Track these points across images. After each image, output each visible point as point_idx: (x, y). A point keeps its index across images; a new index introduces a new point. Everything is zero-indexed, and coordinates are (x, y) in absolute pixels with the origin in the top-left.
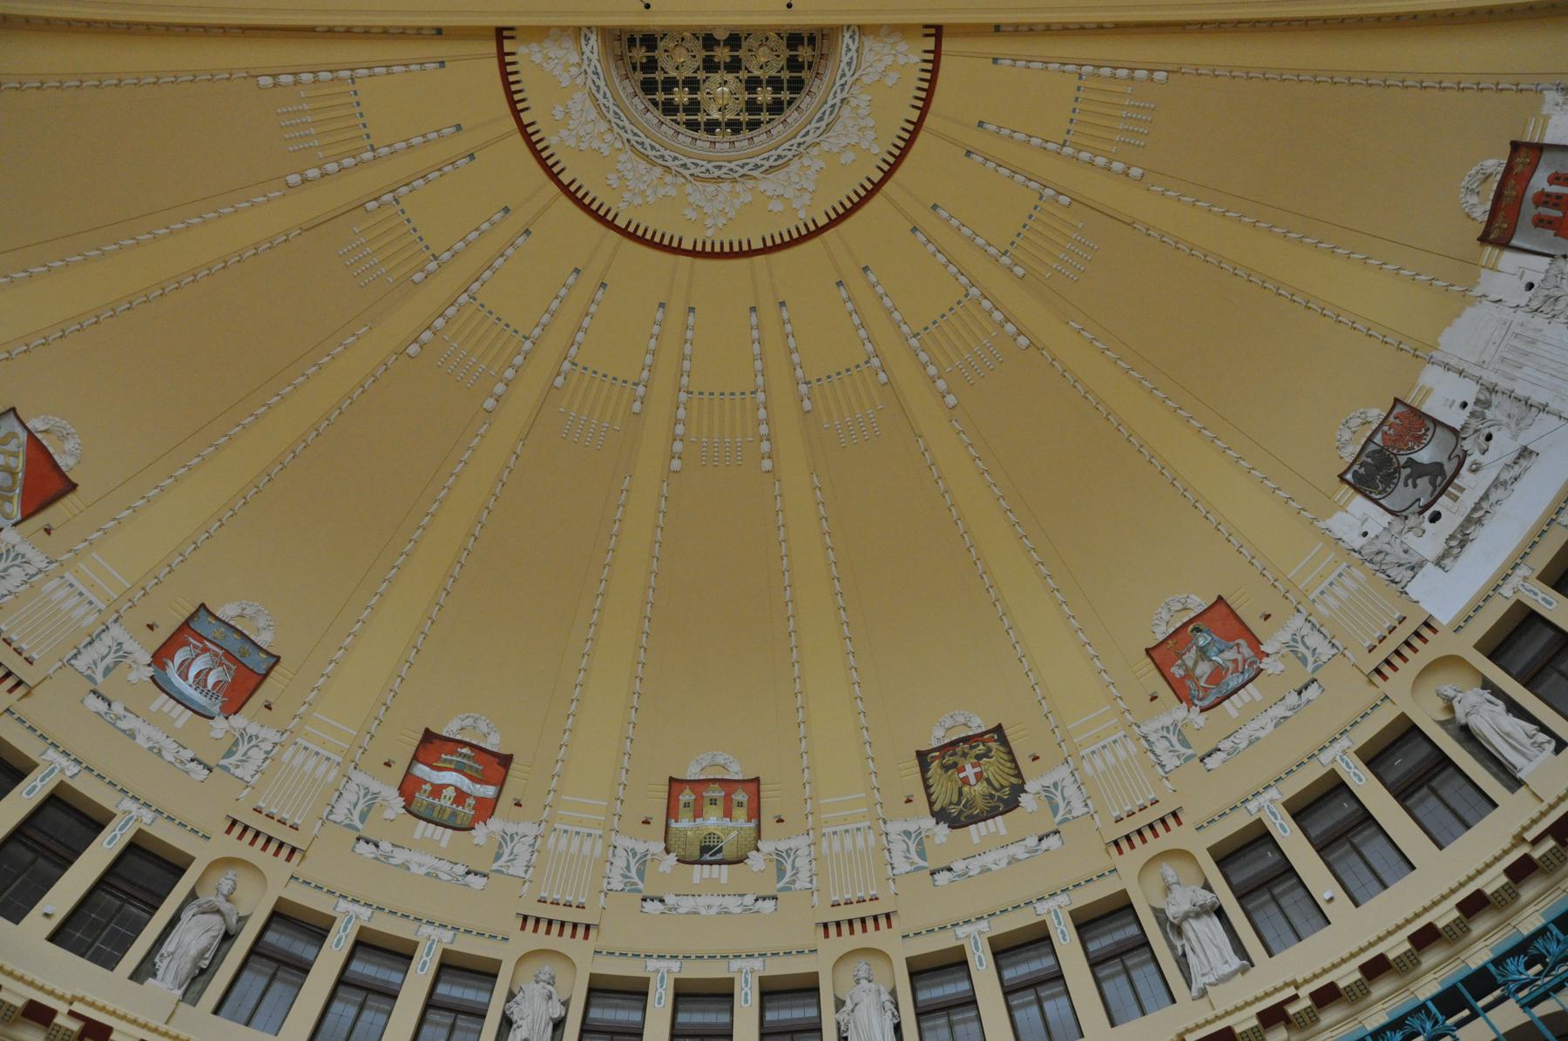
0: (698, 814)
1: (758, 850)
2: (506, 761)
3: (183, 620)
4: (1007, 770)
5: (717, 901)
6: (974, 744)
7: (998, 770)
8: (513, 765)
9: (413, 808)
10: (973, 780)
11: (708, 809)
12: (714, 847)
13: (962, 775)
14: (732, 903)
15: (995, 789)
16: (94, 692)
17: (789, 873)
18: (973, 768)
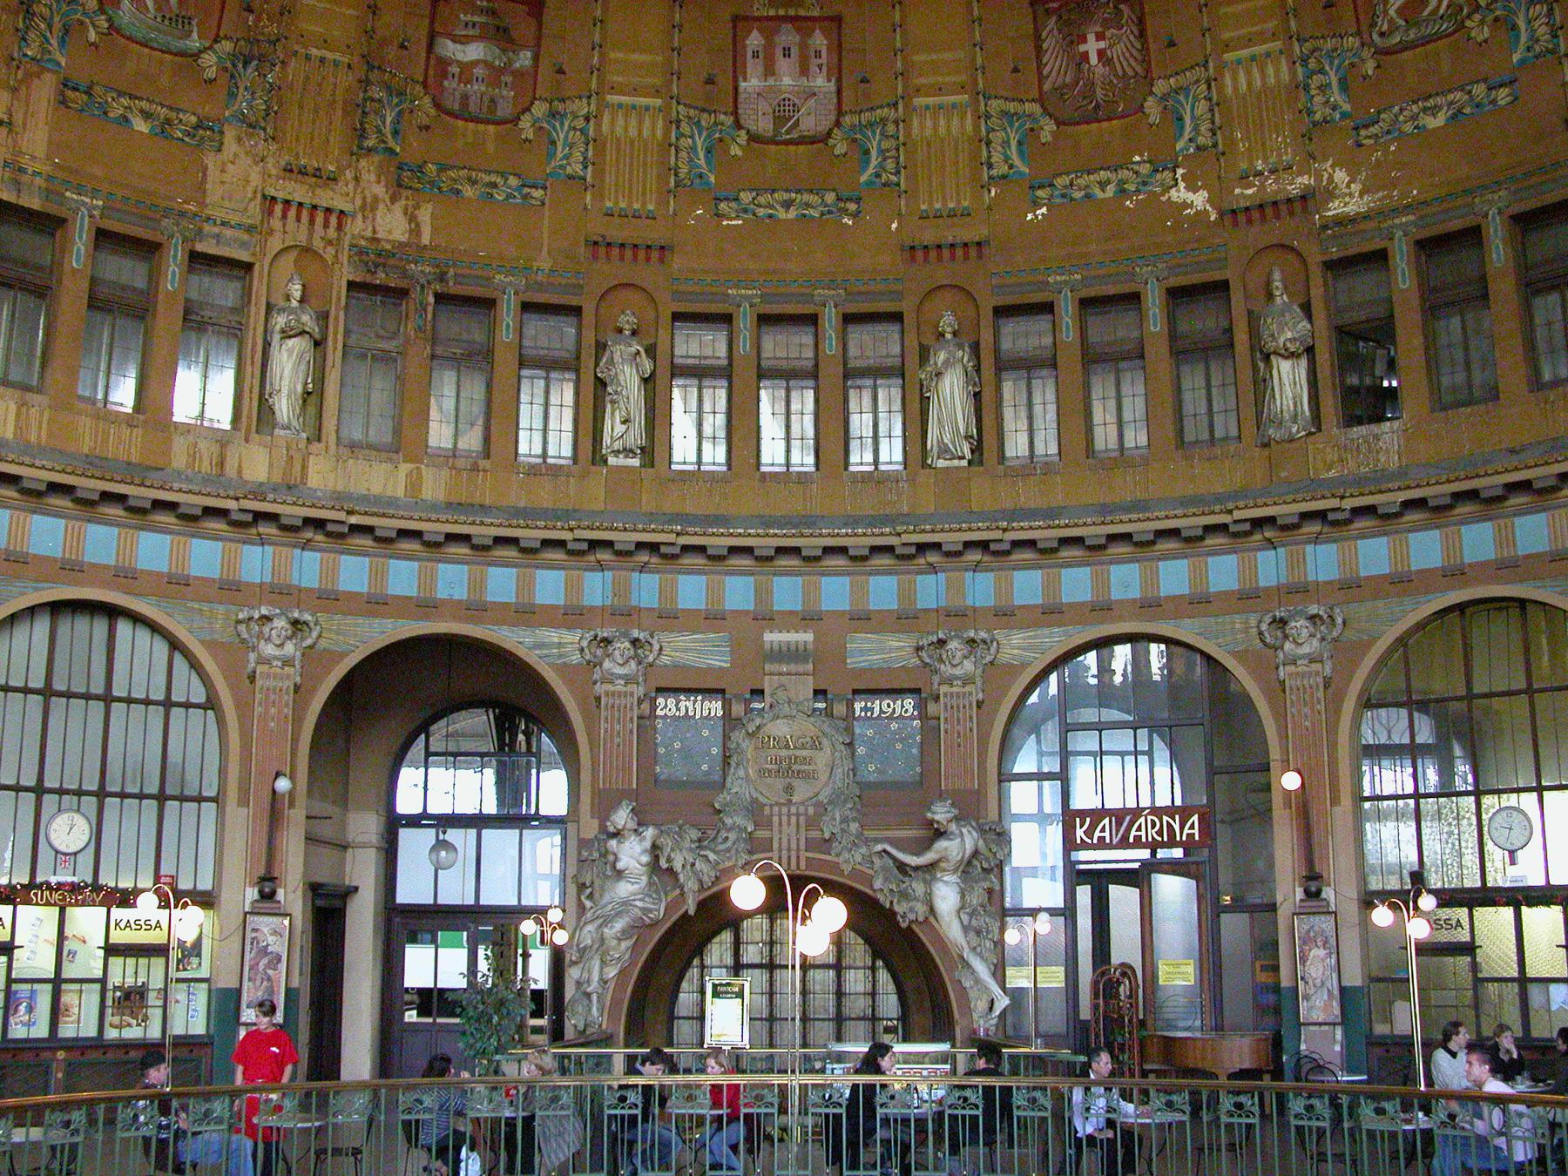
0: (769, 70)
4: (1135, 52)
10: (1094, 60)
11: (783, 64)
12: (791, 118)
18: (1097, 40)
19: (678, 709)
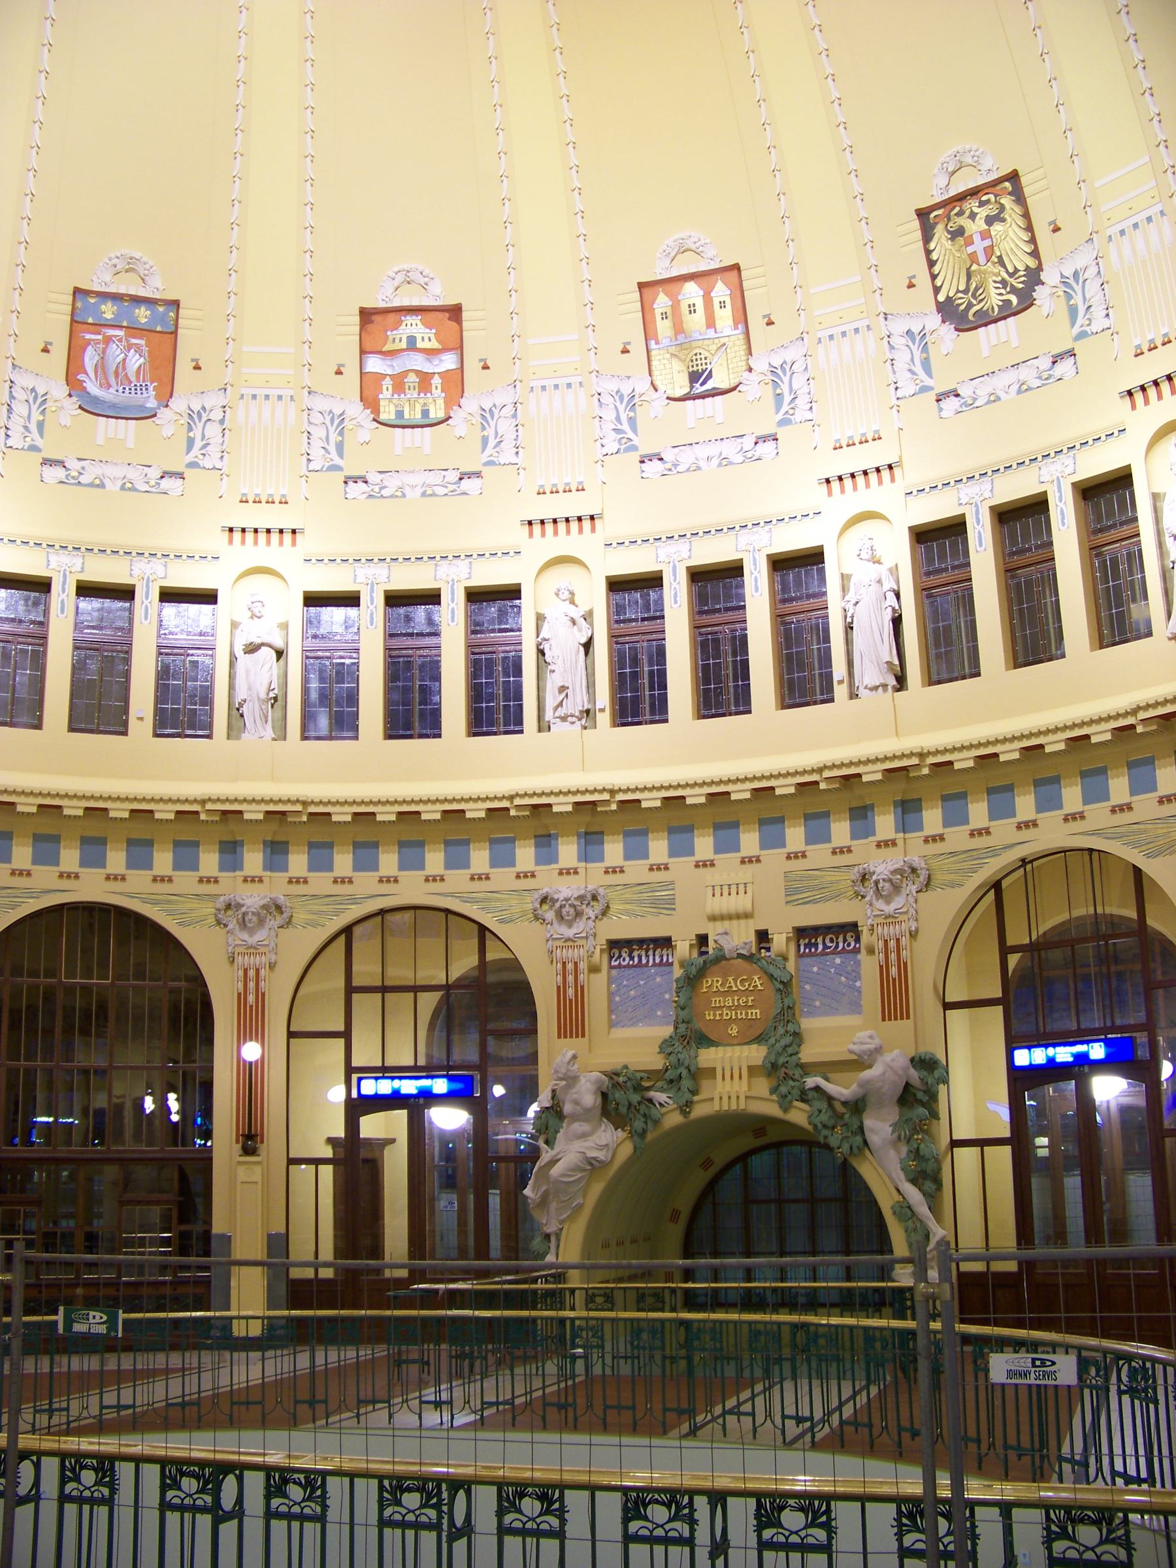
1: (750, 370)
2: (455, 312)
3: (69, 318)
5: (714, 449)
6: (984, 198)
7: (1013, 246)
8: (465, 315)
9: (383, 417)
10: (982, 259)
12: (704, 371)
13: (970, 249)
14: (730, 449)
15: (1011, 275)
16: (46, 462)
17: (787, 398)
19: (632, 958)
